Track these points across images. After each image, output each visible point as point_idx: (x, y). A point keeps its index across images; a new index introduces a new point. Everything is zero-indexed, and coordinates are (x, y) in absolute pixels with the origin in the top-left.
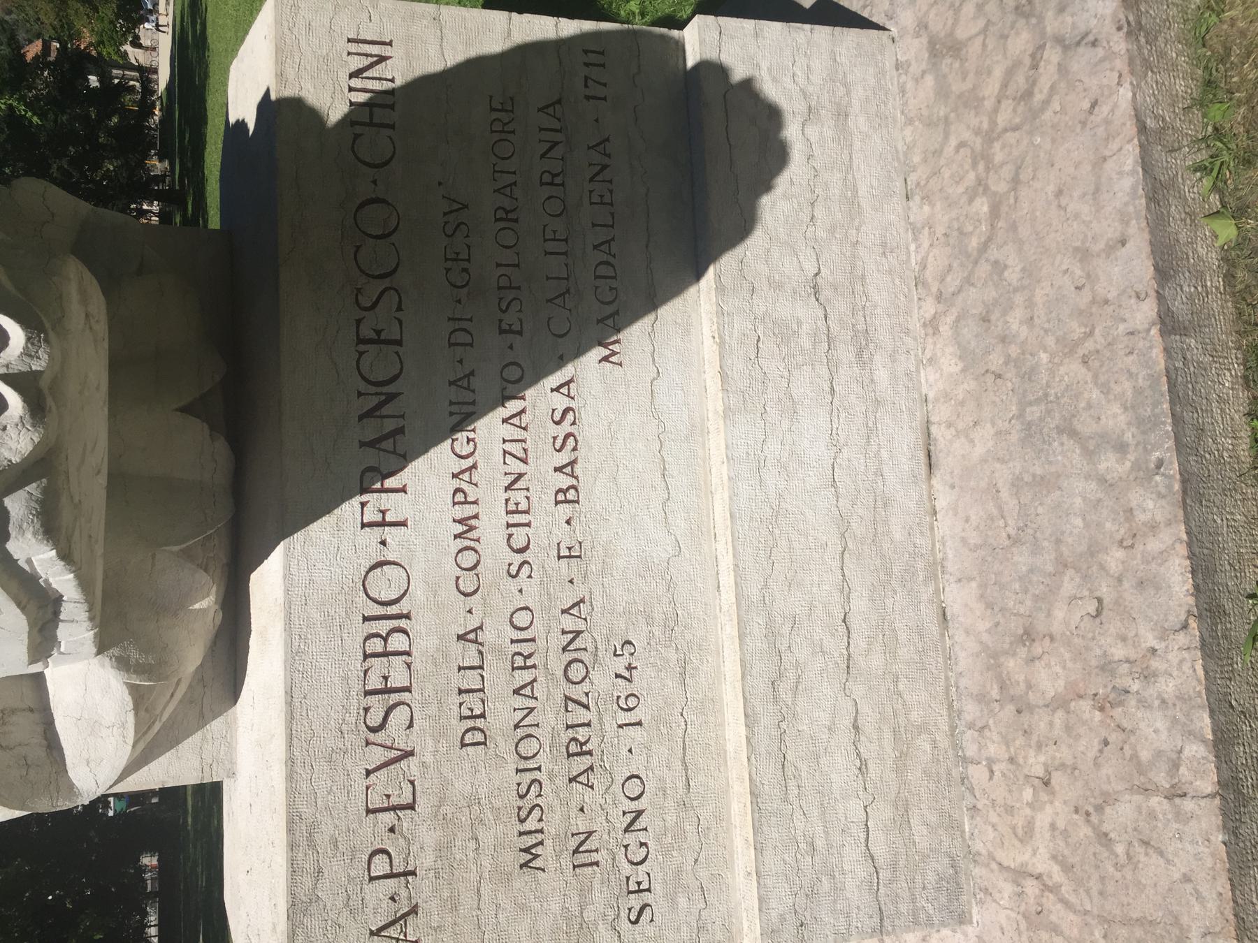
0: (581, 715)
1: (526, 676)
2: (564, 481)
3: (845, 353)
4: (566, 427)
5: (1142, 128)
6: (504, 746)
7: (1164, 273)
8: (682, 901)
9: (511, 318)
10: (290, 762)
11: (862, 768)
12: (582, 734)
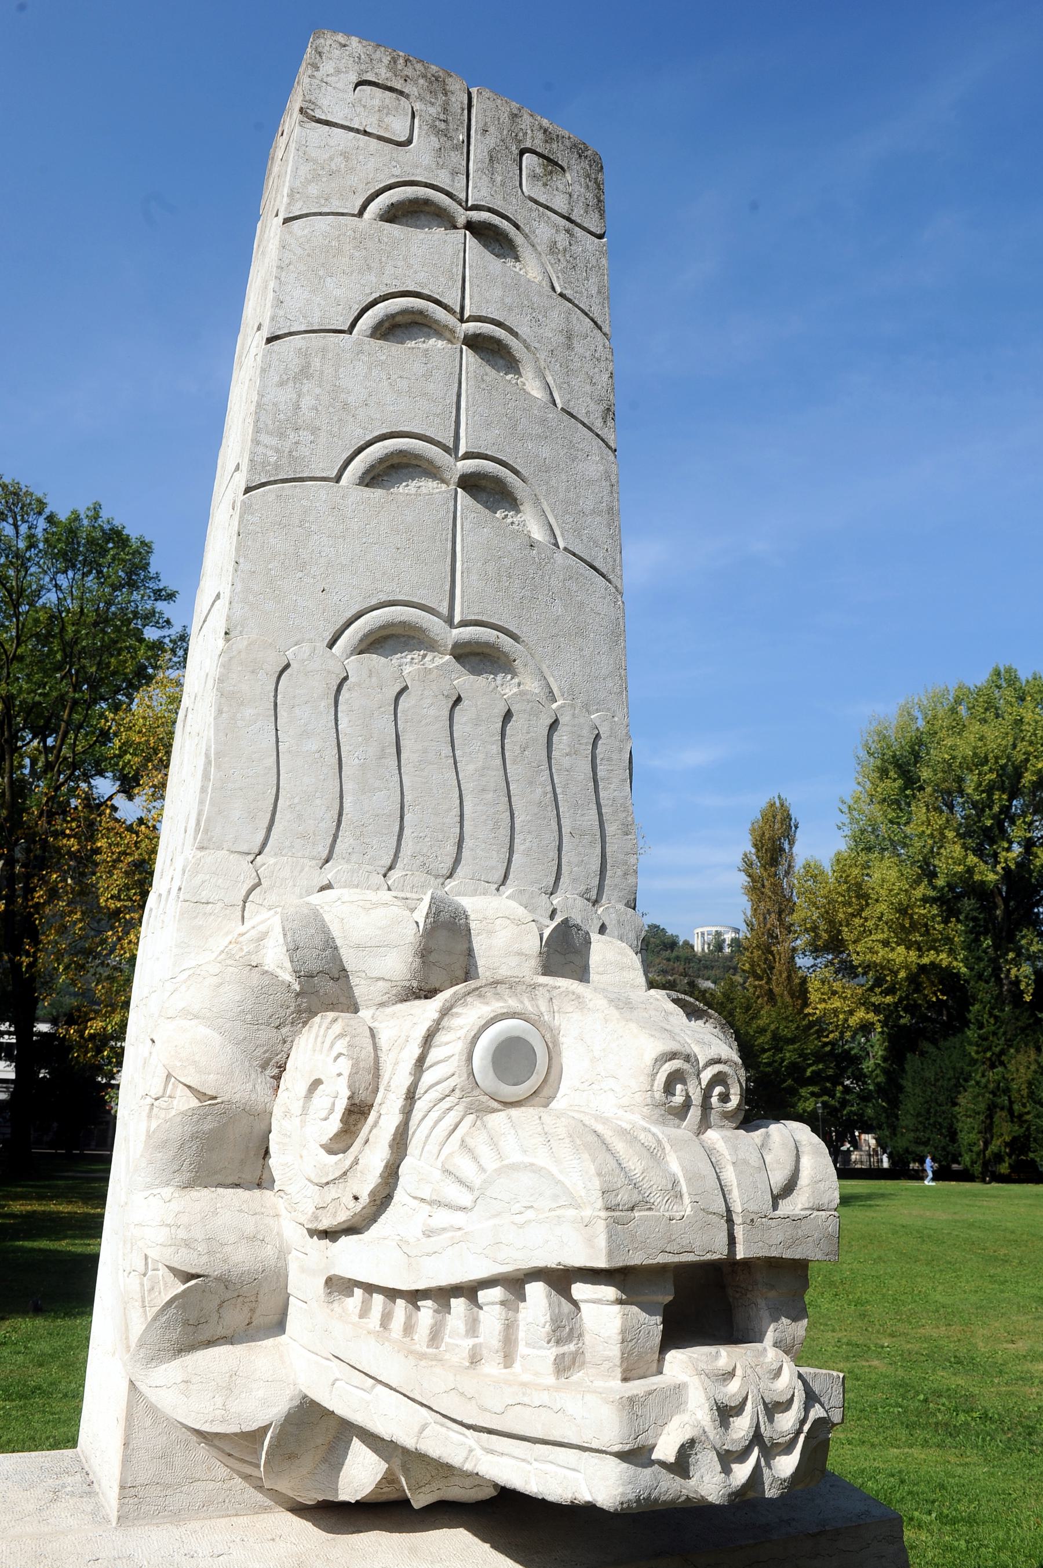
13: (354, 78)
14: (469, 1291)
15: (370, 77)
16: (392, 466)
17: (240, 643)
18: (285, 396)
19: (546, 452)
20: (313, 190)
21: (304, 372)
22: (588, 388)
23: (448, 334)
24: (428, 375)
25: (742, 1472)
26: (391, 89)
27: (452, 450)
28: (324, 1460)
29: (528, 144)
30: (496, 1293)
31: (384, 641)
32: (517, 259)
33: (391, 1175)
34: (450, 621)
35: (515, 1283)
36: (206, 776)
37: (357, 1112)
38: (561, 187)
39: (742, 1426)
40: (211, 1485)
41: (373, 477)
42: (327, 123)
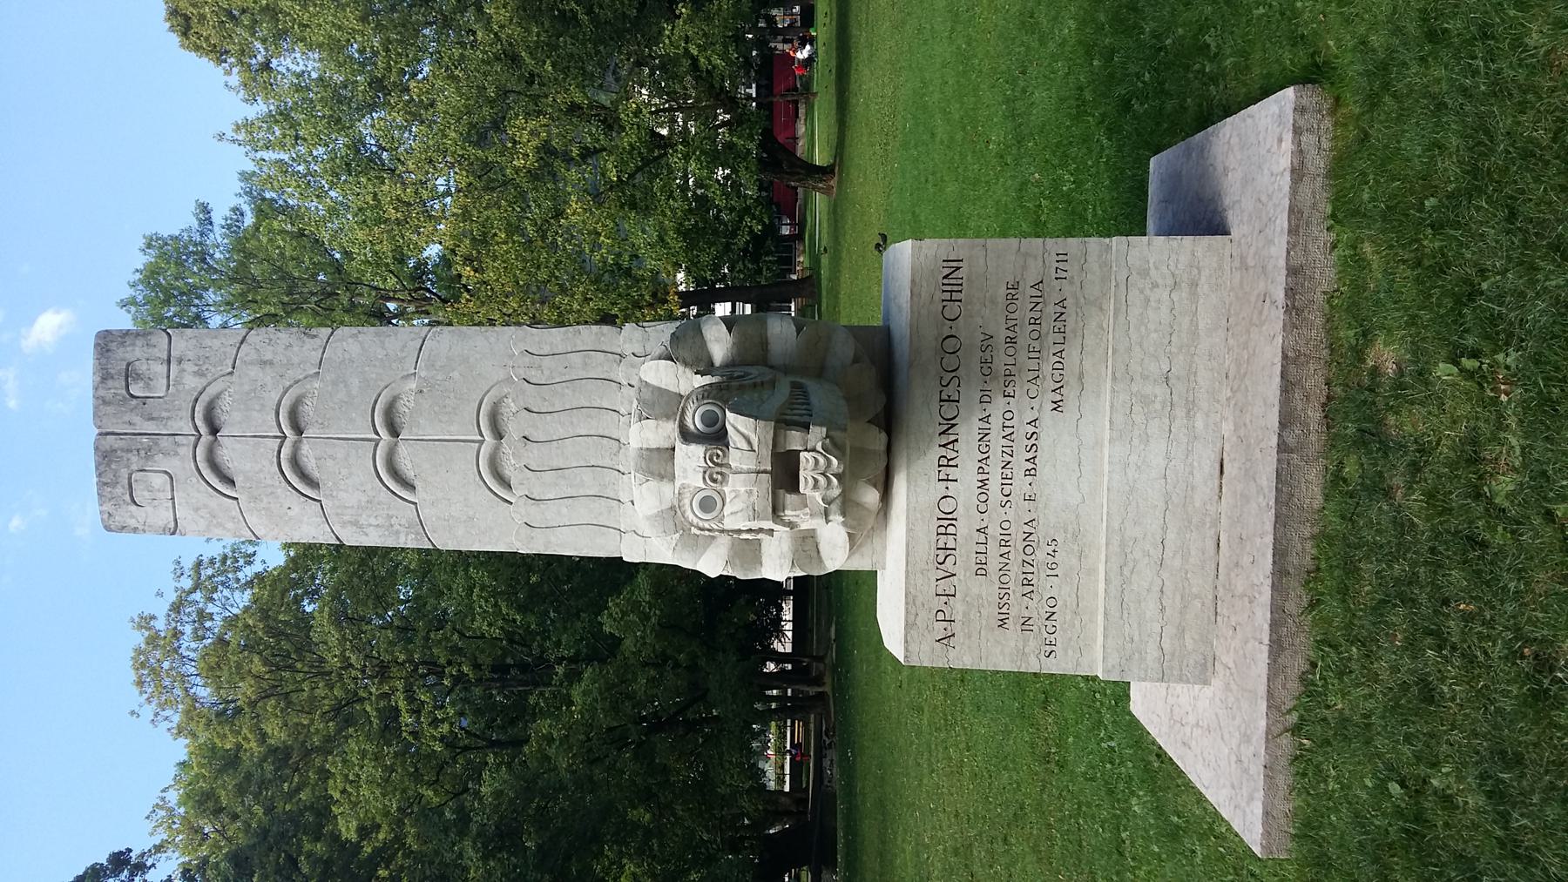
0: (1030, 569)
1: (1006, 550)
2: (1030, 466)
3: (1180, 412)
4: (1032, 441)
5: (1285, 357)
6: (995, 578)
7: (1283, 425)
8: (1070, 652)
9: (1010, 390)
10: (907, 572)
11: (1163, 610)
12: (1029, 577)
15: (127, 497)
19: (355, 382)
22: (296, 349)
25: (835, 480)
34: (481, 442)
38: (145, 367)
39: (821, 479)
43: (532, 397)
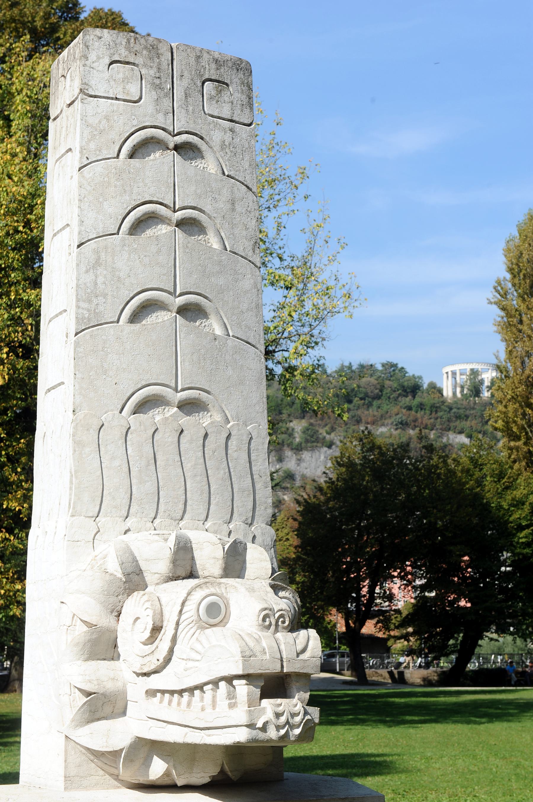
13: (107, 61)
14: (200, 687)
15: (117, 58)
16: (144, 307)
17: (80, 415)
18: (89, 278)
19: (221, 281)
20: (92, 146)
21: (98, 263)
22: (244, 233)
23: (167, 221)
24: (159, 252)
25: (282, 732)
26: (128, 63)
27: (173, 293)
28: (143, 764)
29: (207, 76)
30: (210, 686)
31: (144, 406)
32: (203, 158)
33: (171, 651)
34: (176, 390)
35: (215, 683)
36: (71, 482)
37: (157, 630)
38: (226, 99)
39: (283, 719)
40: (97, 777)
41: (135, 318)
42: (95, 97)
43: (215, 442)
